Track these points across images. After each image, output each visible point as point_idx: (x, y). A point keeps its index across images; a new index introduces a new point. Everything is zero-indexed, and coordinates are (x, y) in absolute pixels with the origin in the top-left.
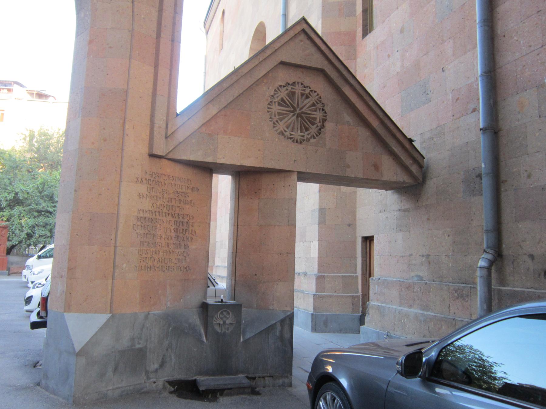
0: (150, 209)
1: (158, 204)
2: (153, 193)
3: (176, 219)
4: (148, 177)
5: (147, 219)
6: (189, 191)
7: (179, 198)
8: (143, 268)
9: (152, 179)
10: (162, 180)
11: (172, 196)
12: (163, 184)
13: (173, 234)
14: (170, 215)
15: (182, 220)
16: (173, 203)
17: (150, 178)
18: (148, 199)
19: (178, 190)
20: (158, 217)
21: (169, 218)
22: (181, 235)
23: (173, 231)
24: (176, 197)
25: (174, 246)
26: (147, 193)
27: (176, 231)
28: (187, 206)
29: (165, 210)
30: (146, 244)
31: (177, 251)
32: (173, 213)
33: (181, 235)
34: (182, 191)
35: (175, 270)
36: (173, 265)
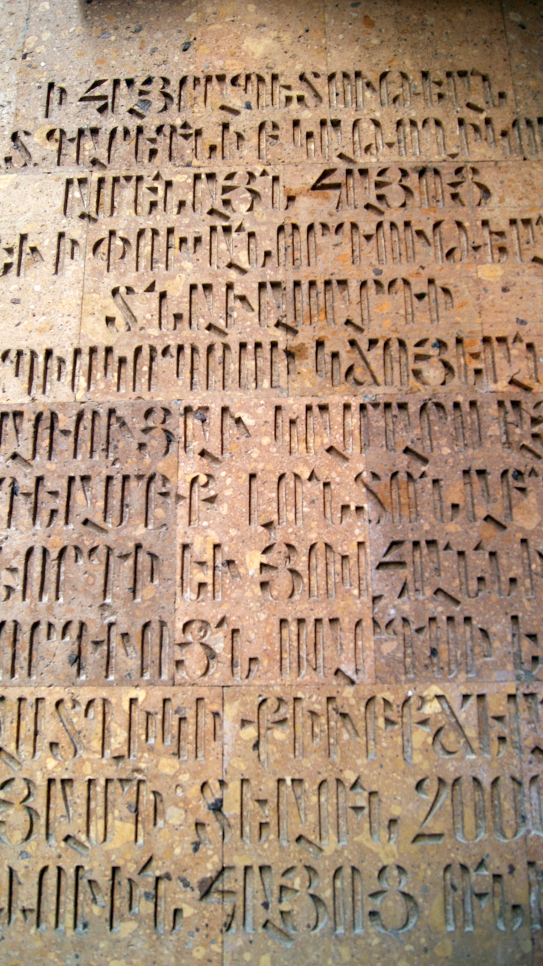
0: (101, 337)
1: (177, 290)
2: (125, 221)
3: (381, 393)
4: (72, 117)
5: (66, 422)
6: (478, 151)
7: (395, 215)
8: (26, 896)
9: (108, 123)
10: (204, 115)
11: (306, 210)
12: (212, 135)
13: (365, 533)
14: (305, 366)
15: (458, 390)
16: (330, 258)
17: (91, 117)
18: (72, 268)
19: (363, 160)
20: (171, 389)
21: (299, 389)
22: (453, 529)
23: (355, 496)
24: (347, 216)
25: (390, 646)
26: (76, 229)
27: (386, 490)
28: (491, 271)
29: (246, 326)
30: (59, 648)
31: (435, 696)
32: (338, 342)
33: (453, 529)
34: (410, 161)
35: (433, 910)
36: (386, 849)
